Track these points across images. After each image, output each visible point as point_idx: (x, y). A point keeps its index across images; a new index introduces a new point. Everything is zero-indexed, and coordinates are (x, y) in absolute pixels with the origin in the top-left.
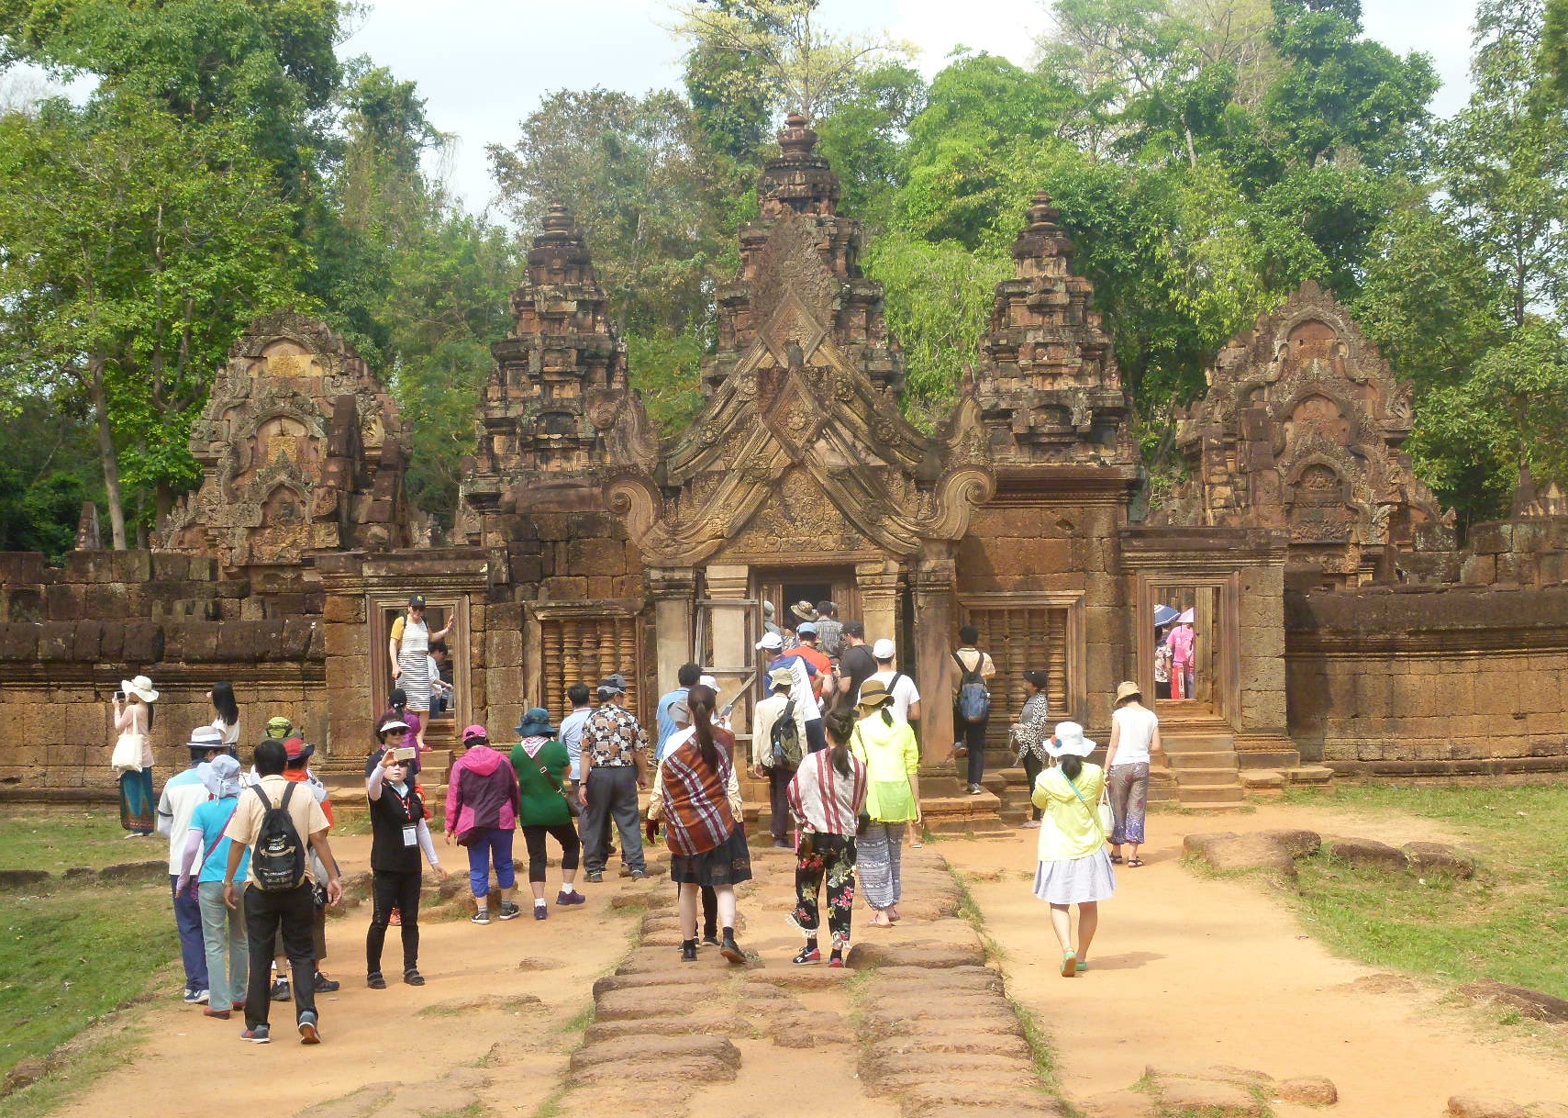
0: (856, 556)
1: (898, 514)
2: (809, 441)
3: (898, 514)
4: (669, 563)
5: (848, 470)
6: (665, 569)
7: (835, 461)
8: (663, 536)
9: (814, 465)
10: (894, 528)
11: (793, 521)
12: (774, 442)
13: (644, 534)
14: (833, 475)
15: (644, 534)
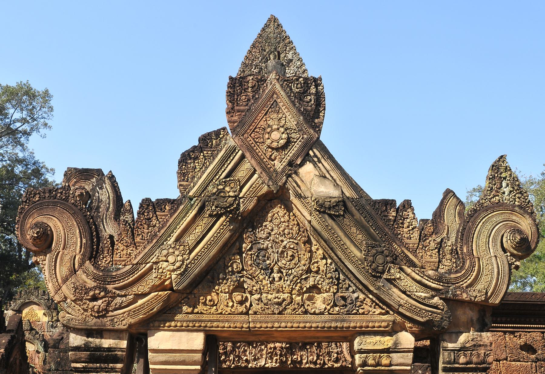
0: (355, 321)
1: (412, 264)
2: (291, 164)
3: (412, 264)
4: (92, 322)
5: (343, 202)
6: (89, 333)
7: (327, 190)
8: (91, 283)
9: (299, 196)
10: (406, 283)
11: (269, 270)
12: (246, 166)
13: (65, 280)
14: (324, 208)
15: (65, 280)
